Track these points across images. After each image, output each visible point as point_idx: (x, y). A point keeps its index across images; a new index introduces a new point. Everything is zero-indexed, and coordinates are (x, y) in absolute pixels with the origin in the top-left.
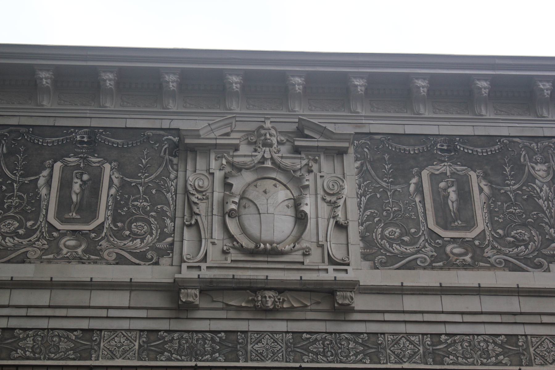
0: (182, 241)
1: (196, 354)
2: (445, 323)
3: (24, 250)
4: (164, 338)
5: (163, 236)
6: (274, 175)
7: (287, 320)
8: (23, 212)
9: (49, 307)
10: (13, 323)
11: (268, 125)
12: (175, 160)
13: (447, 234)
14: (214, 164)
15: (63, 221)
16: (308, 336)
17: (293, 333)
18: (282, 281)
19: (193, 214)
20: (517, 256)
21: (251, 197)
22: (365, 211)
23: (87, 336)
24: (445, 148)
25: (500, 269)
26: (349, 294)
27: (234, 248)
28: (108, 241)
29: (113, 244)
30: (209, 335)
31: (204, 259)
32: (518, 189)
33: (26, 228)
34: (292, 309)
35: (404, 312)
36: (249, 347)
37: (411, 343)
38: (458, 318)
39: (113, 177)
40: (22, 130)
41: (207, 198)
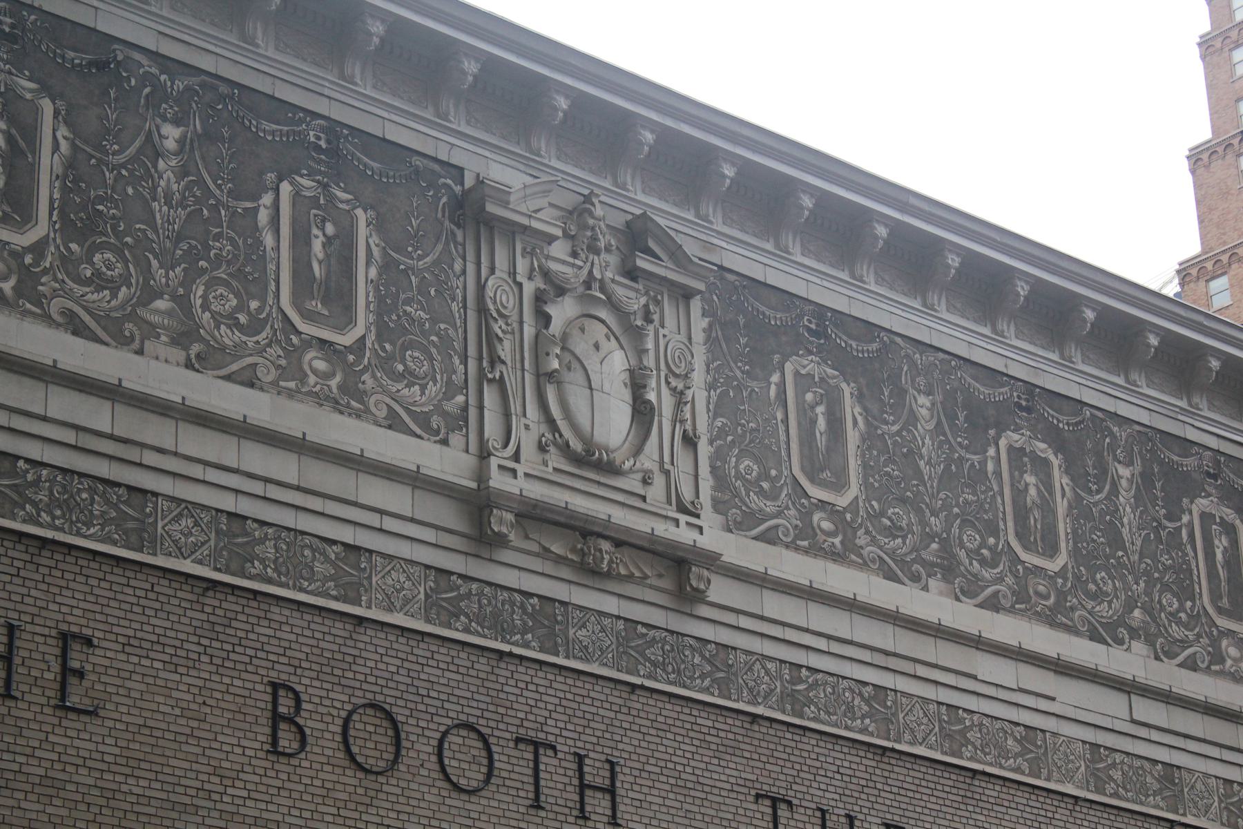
0: (481, 408)
1: (503, 630)
2: (808, 648)
3: (250, 360)
4: (458, 588)
5: (450, 390)
6: (603, 314)
7: (620, 596)
8: (240, 274)
9: (298, 488)
10: (246, 507)
11: (599, 211)
12: (459, 235)
13: (816, 493)
14: (522, 266)
15: (308, 316)
16: (644, 631)
17: (626, 620)
18: (628, 530)
19: (495, 360)
20: (892, 553)
21: (578, 351)
22: (716, 416)
23: (352, 557)
24: (813, 326)
25: (873, 570)
26: (706, 573)
27: (555, 444)
28: (374, 376)
29: (381, 386)
30: (517, 597)
31: (516, 457)
32: (898, 433)
33: (249, 313)
34: (630, 578)
35: (762, 618)
36: (571, 632)
37: (767, 672)
38: (822, 644)
39: (371, 241)
40: (224, 89)
41: (513, 333)
